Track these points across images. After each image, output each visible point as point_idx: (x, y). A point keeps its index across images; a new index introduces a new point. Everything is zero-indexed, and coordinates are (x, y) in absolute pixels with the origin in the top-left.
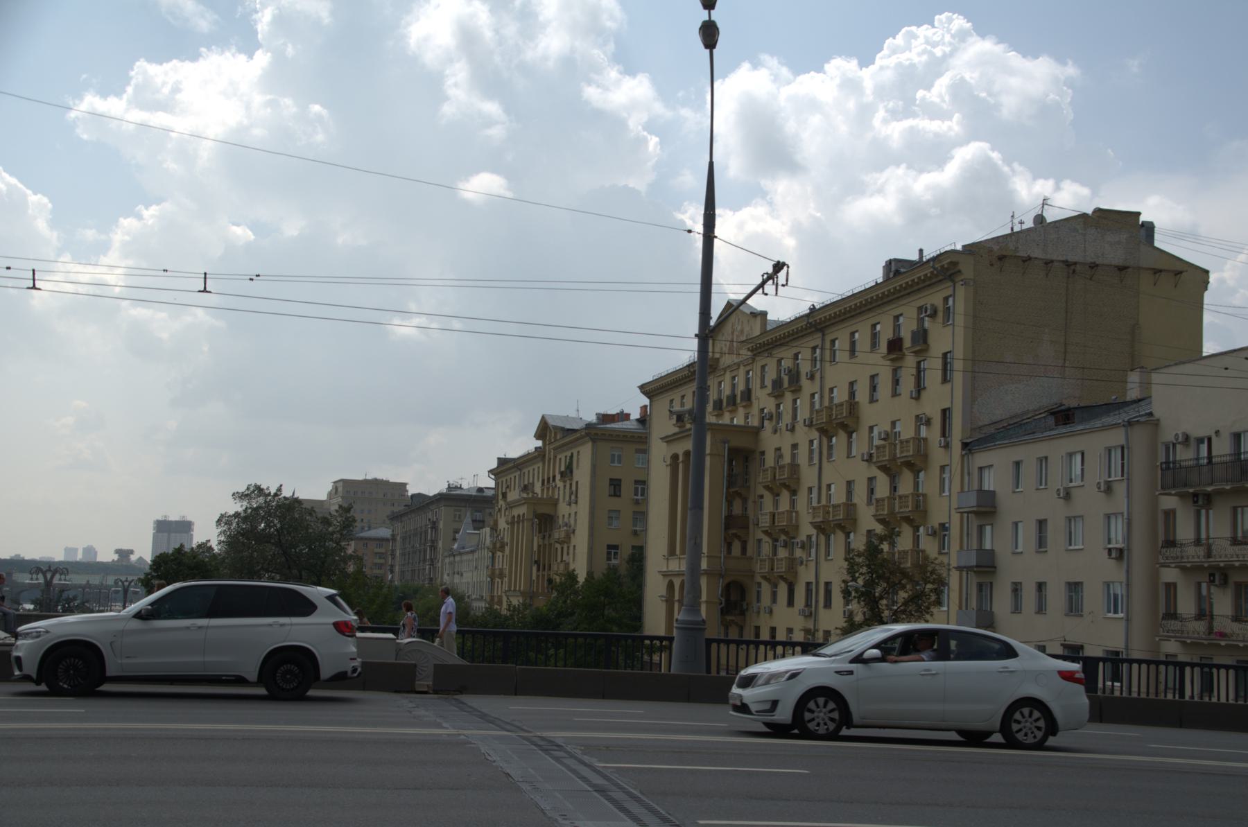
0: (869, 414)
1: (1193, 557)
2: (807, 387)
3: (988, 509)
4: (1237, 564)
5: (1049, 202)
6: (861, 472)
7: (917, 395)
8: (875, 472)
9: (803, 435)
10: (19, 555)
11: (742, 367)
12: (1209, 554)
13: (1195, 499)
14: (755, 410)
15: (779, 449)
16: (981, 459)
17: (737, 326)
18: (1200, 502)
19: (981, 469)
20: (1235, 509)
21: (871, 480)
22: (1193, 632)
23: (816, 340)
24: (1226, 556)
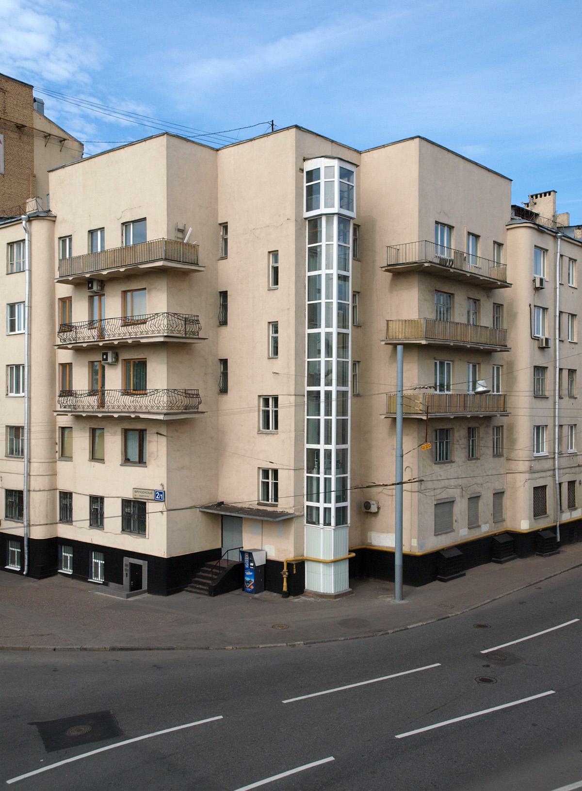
4: (130, 341)
12: (101, 336)
13: (90, 285)
18: (95, 288)
20: (125, 293)
24: (119, 334)
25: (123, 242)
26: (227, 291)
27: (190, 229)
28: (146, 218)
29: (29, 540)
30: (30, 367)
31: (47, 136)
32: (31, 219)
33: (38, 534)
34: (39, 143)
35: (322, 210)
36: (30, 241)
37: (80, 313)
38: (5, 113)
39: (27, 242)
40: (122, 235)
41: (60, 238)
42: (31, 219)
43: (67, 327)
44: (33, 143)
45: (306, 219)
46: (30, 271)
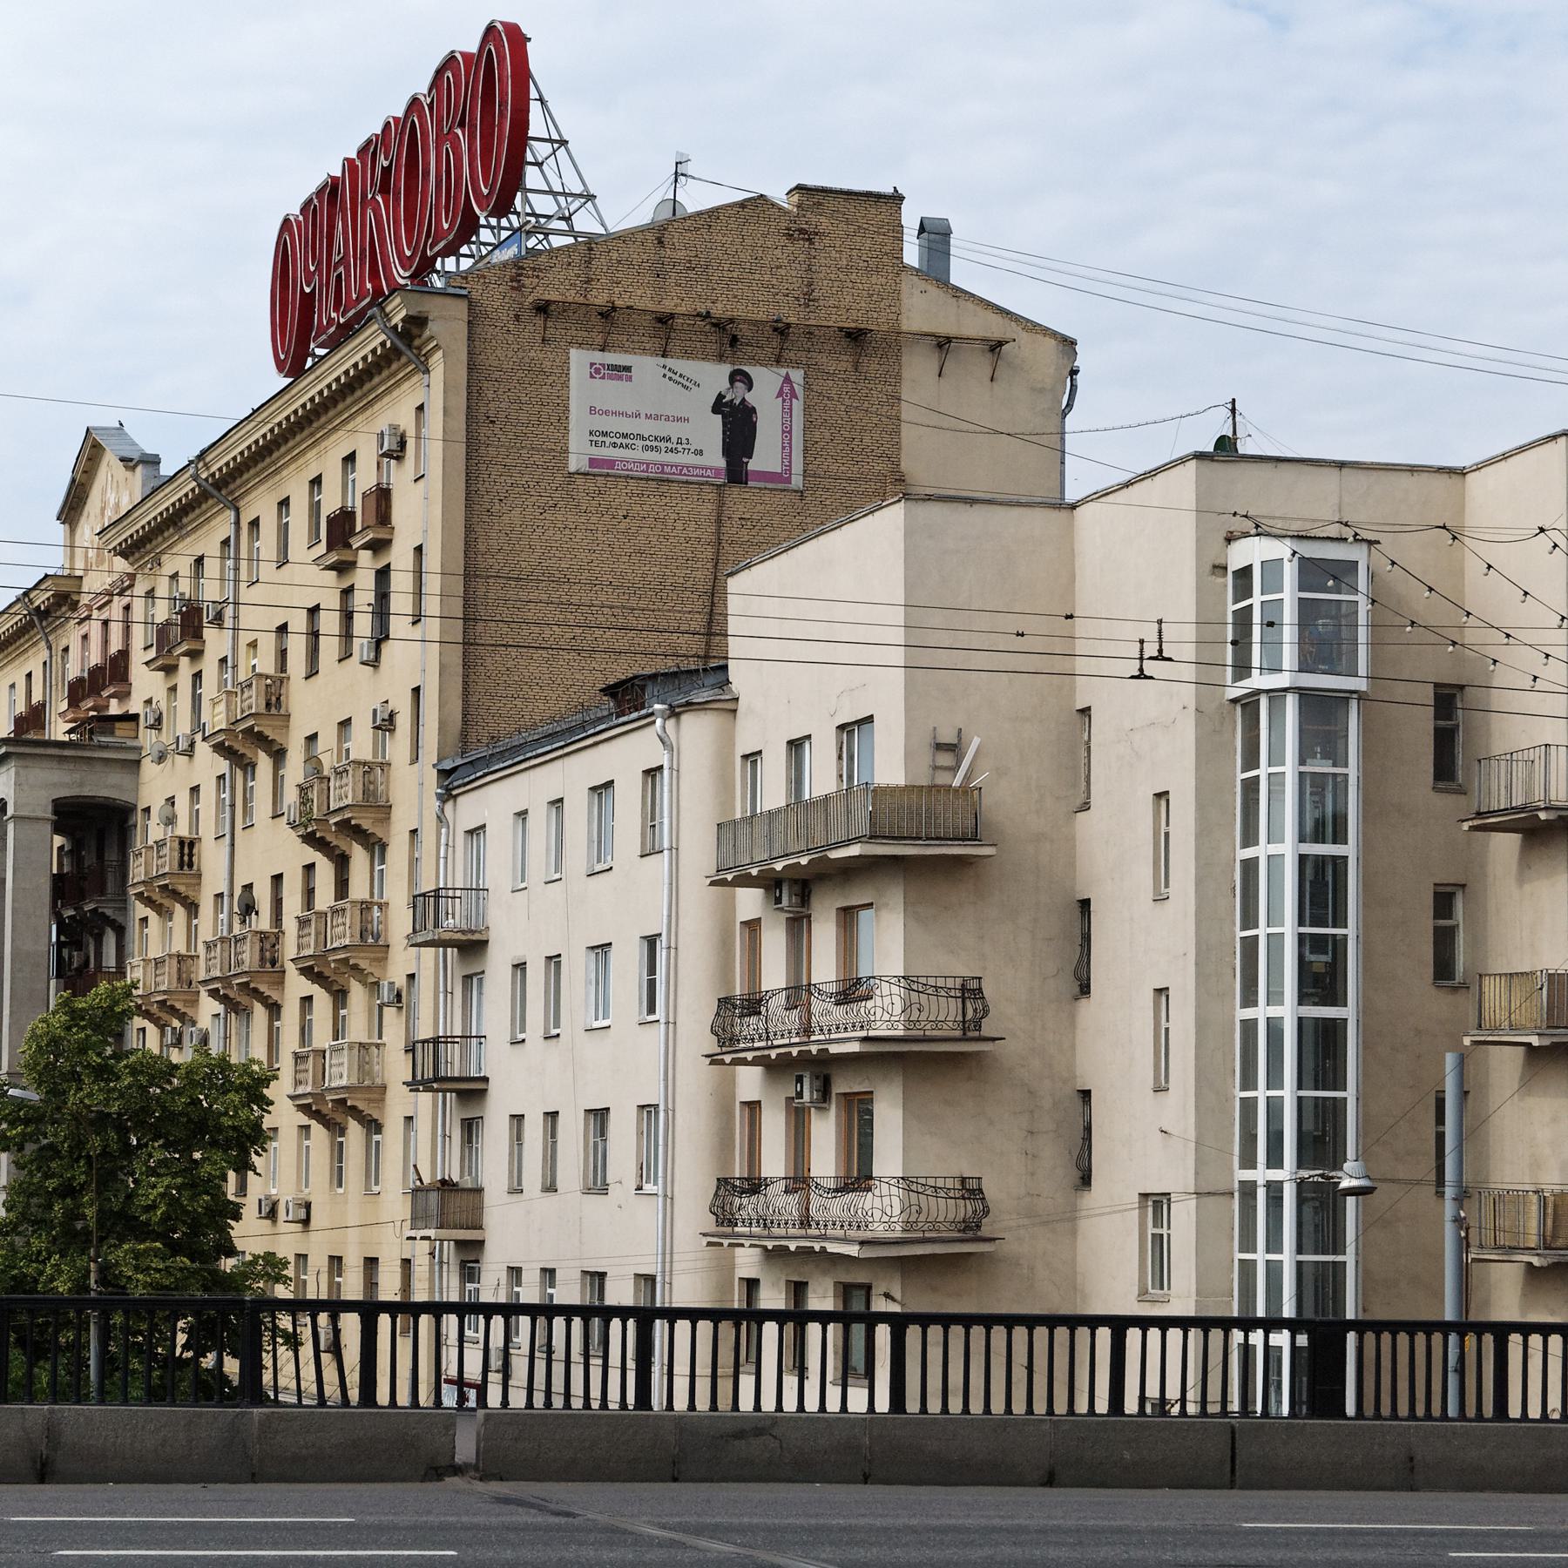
6: (290, 853)
7: (372, 655)
9: (208, 764)
11: (116, 598)
15: (171, 801)
16: (471, 808)
17: (108, 495)
21: (309, 868)
23: (222, 526)
25: (841, 776)
26: (1089, 899)
27: (976, 741)
28: (872, 716)
30: (671, 1112)
31: (943, 343)
32: (677, 710)
34: (918, 369)
35: (1258, 681)
36: (676, 771)
38: (808, 299)
40: (840, 757)
41: (745, 757)
42: (677, 710)
44: (898, 376)
45: (1234, 701)
46: (675, 849)
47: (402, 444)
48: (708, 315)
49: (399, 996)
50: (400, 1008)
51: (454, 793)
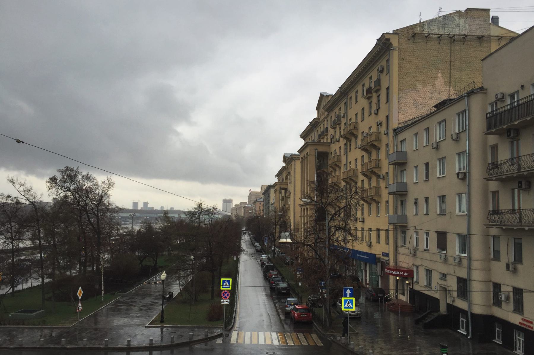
0: (363, 127)
1: (507, 171)
2: (343, 121)
3: (402, 161)
5: (442, 10)
7: (377, 112)
8: (364, 153)
9: (343, 142)
10: (153, 208)
11: (326, 119)
12: (519, 169)
14: (329, 136)
15: (335, 150)
19: (401, 141)
21: (363, 156)
22: (507, 221)
24: (528, 167)
29: (473, 315)
33: (478, 310)
37: (504, 155)
39: (467, 112)
43: (495, 165)
47: (383, 69)
48: (449, 34)
49: (384, 177)
50: (384, 179)
51: (397, 134)
